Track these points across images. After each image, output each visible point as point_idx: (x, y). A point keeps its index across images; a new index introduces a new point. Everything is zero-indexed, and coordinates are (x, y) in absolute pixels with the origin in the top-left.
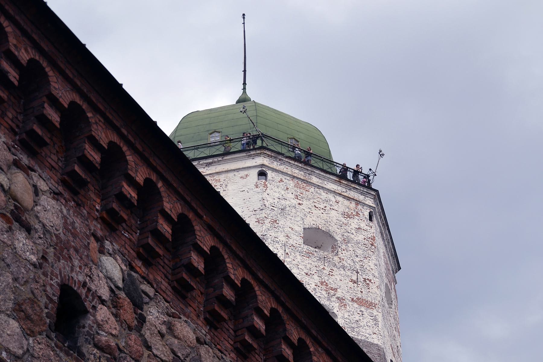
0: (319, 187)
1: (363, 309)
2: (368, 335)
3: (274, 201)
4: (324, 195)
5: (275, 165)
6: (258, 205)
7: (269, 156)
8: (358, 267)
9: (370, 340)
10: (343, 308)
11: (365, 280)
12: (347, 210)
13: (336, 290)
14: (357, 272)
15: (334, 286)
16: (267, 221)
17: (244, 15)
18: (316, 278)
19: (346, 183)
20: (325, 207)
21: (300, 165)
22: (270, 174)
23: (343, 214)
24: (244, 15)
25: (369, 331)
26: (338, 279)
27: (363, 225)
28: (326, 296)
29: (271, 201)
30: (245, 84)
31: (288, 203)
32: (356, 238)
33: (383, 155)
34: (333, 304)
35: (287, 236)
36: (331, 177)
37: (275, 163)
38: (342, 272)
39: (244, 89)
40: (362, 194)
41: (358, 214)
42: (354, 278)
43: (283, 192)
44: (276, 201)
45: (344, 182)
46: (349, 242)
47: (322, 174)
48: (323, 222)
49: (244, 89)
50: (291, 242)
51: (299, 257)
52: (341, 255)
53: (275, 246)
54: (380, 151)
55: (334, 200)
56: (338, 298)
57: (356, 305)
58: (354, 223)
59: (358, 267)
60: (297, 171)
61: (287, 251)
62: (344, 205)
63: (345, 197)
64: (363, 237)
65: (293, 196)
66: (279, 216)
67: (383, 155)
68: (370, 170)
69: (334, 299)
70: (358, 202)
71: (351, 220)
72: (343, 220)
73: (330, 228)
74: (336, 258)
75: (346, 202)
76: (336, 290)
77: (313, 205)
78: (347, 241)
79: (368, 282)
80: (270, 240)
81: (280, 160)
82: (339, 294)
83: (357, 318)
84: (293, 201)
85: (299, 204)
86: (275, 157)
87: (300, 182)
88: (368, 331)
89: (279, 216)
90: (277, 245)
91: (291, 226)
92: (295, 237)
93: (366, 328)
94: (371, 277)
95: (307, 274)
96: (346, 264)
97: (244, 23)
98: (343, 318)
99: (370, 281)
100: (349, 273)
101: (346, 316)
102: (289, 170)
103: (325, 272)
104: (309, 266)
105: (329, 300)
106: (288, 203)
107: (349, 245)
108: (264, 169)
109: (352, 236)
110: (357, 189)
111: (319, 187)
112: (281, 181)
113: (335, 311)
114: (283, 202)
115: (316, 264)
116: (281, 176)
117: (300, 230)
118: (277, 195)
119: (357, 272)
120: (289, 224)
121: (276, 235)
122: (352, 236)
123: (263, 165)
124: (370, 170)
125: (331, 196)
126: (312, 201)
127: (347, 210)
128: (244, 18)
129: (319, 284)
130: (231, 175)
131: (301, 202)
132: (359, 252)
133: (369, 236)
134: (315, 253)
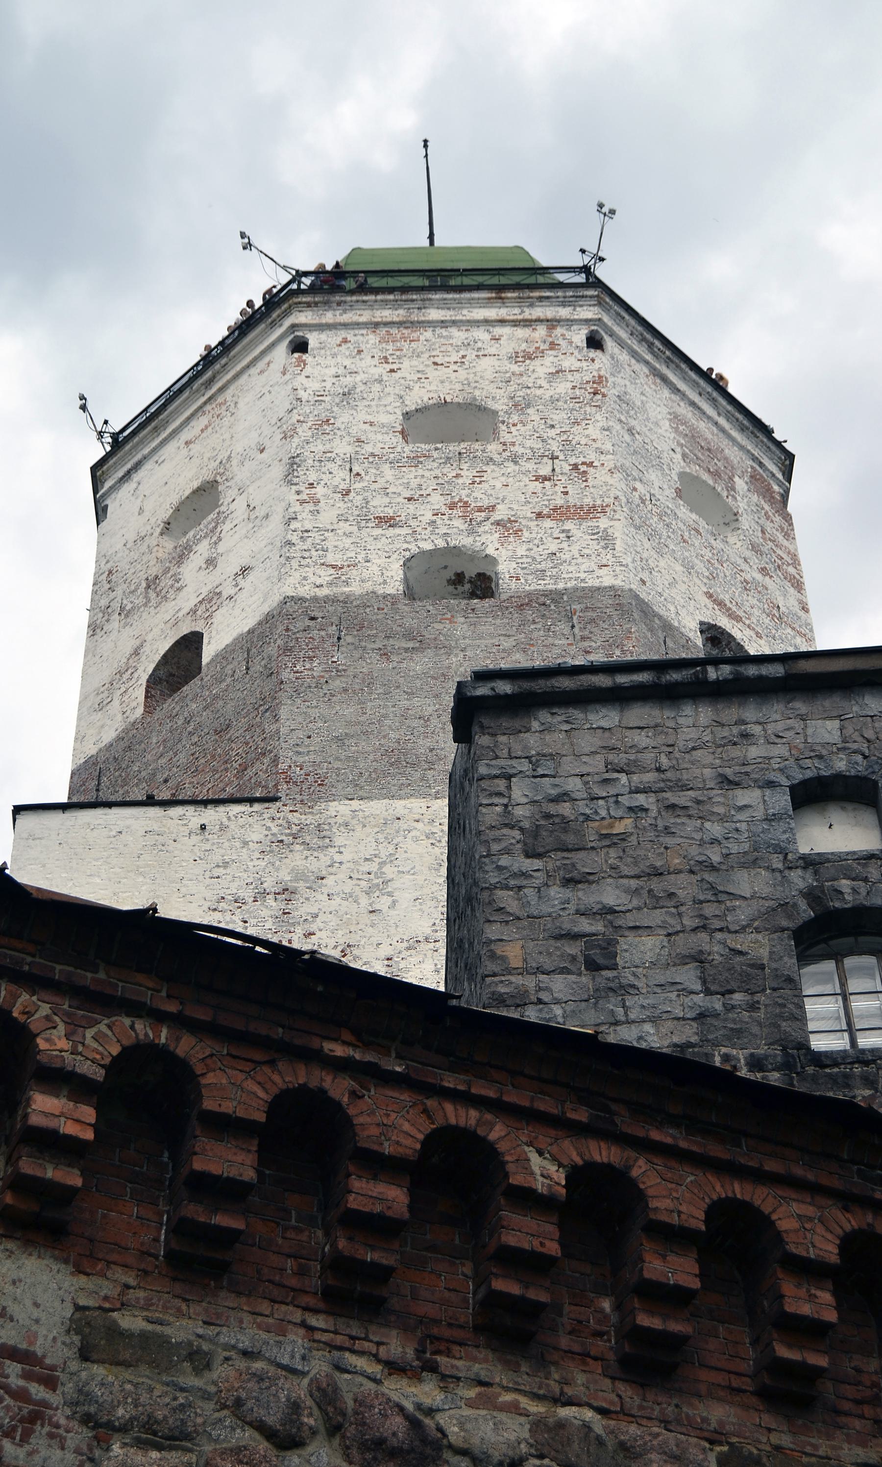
0: (443, 324)
2: (583, 575)
4: (458, 335)
7: (309, 305)
8: (554, 446)
9: (592, 582)
10: (511, 539)
11: (575, 467)
12: (524, 346)
13: (492, 508)
15: (486, 503)
17: (426, 141)
18: (437, 501)
19: (515, 295)
20: (463, 357)
21: (391, 297)
22: (313, 339)
23: (515, 357)
24: (426, 141)
25: (586, 565)
27: (569, 363)
29: (315, 385)
32: (551, 393)
33: (612, 212)
34: (483, 539)
36: (475, 295)
38: (511, 467)
40: (563, 304)
41: (553, 346)
42: (545, 471)
44: (328, 385)
45: (509, 295)
46: (528, 406)
47: (451, 296)
52: (505, 437)
53: (323, 469)
54: (601, 206)
55: (486, 336)
56: (497, 523)
57: (548, 523)
58: (542, 367)
61: (356, 468)
62: (513, 339)
64: (569, 385)
66: (335, 409)
67: (612, 212)
68: (583, 251)
69: (487, 526)
70: (552, 323)
71: (537, 362)
72: (515, 368)
73: (477, 393)
74: (493, 448)
75: (521, 332)
76: (492, 508)
77: (430, 363)
78: (520, 406)
79: (583, 468)
80: (310, 461)
83: (553, 547)
84: (373, 370)
85: (392, 371)
86: (326, 303)
87: (394, 331)
88: (583, 567)
89: (335, 409)
90: (330, 465)
91: (369, 418)
92: (380, 437)
93: (580, 560)
94: (592, 457)
95: (409, 499)
96: (520, 450)
97: (426, 156)
98: (513, 558)
100: (530, 466)
102: (365, 316)
103: (460, 481)
104: (414, 483)
105: (471, 532)
109: (539, 392)
110: (548, 298)
111: (443, 324)
112: (345, 341)
113: (490, 551)
115: (437, 472)
116: (343, 334)
117: (395, 419)
119: (553, 458)
120: (363, 416)
121: (328, 447)
122: (539, 392)
123: (294, 327)
124: (583, 251)
125: (481, 334)
126: (426, 355)
127: (524, 346)
129: (444, 509)
131: (395, 367)
132: (557, 417)
134: (435, 454)
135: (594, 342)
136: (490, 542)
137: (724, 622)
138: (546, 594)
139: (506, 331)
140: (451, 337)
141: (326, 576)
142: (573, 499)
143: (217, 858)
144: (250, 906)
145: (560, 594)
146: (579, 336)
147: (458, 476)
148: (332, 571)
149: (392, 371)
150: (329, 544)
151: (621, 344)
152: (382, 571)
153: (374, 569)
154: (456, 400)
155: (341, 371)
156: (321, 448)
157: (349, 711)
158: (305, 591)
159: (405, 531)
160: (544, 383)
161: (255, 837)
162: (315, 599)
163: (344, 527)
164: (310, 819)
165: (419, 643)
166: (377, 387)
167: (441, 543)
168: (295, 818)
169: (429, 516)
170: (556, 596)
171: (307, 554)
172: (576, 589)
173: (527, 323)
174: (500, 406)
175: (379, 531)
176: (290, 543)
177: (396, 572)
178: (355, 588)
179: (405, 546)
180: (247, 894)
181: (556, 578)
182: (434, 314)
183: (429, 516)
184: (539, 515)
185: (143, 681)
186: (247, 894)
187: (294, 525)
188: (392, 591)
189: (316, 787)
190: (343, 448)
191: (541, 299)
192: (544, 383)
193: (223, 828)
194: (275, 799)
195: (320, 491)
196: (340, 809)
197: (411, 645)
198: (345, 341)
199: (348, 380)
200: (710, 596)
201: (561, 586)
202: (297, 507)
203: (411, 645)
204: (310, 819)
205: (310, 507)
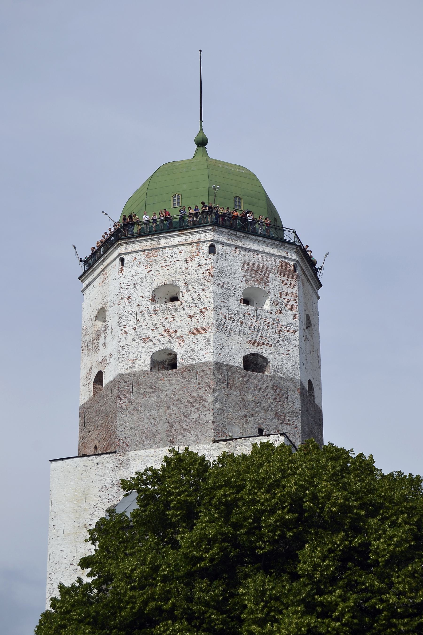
1: (198, 337)
2: (201, 357)
3: (129, 280)
5: (132, 247)
6: (118, 290)
7: (124, 243)
9: (203, 360)
10: (181, 344)
14: (196, 307)
15: (174, 329)
16: (123, 301)
18: (161, 329)
19: (187, 232)
25: (202, 353)
26: (179, 321)
27: (203, 261)
28: (168, 340)
30: (201, 121)
31: (140, 275)
32: (196, 276)
34: (172, 345)
35: (139, 305)
37: (131, 245)
39: (201, 126)
40: (202, 232)
42: (192, 313)
43: (136, 269)
44: (130, 280)
45: (185, 232)
46: (189, 284)
48: (169, 276)
49: (201, 126)
50: (142, 308)
51: (147, 318)
53: (129, 319)
56: (177, 338)
57: (192, 336)
58: (194, 264)
59: (196, 301)
60: (148, 243)
61: (138, 318)
63: (187, 244)
64: (202, 272)
65: (144, 268)
66: (132, 291)
69: (175, 339)
70: (198, 243)
71: (193, 262)
72: (186, 266)
75: (189, 248)
77: (160, 266)
78: (186, 284)
79: (204, 310)
80: (125, 316)
81: (133, 241)
82: (178, 334)
83: (193, 346)
85: (149, 272)
87: (150, 252)
88: (201, 354)
89: (132, 291)
90: (131, 317)
92: (145, 302)
93: (200, 351)
95: (153, 330)
97: (201, 60)
99: (205, 309)
101: (184, 349)
105: (170, 342)
106: (140, 275)
107: (189, 286)
108: (122, 256)
110: (197, 231)
112: (135, 259)
113: (175, 350)
114: (136, 277)
115: (161, 317)
118: (131, 274)
121: (130, 309)
122: (192, 276)
123: (120, 254)
125: (176, 250)
126: (159, 263)
128: (201, 54)
129: (163, 334)
130: (107, 270)
131: (150, 269)
132: (198, 287)
133: (207, 268)
135: (212, 249)
136: (175, 347)
137: (254, 350)
138: (190, 366)
139: (183, 248)
140: (167, 253)
141: (129, 364)
142: (200, 325)
143: (101, 473)
144: (110, 489)
145: (194, 365)
146: (206, 248)
147: (167, 318)
148: (131, 362)
149: (149, 272)
150: (130, 351)
151: (222, 244)
152: (145, 363)
153: (143, 360)
154: (168, 283)
155: (134, 273)
156: (128, 310)
157: (135, 417)
158: (123, 372)
159: (151, 343)
160: (194, 272)
161: (111, 465)
162: (126, 374)
163: (134, 344)
164: (124, 458)
165: (155, 389)
166: (144, 280)
167: (161, 348)
168: (121, 458)
169: (158, 337)
170: (192, 366)
171: (124, 356)
172: (198, 363)
173: (190, 244)
174: (180, 284)
175: (144, 344)
176: (119, 352)
177: (149, 361)
178: (137, 369)
179: (151, 350)
180: (109, 485)
181: (193, 359)
182: (163, 242)
183: (158, 337)
184: (190, 333)
185: (93, 381)
186: (109, 485)
187: (121, 344)
188: (147, 369)
189: (126, 447)
190: (134, 309)
191: (195, 232)
192: (194, 272)
193: (103, 463)
194: (115, 452)
195: (128, 328)
196: (132, 454)
197: (152, 390)
198: (135, 259)
199: (136, 277)
200: (250, 342)
201: (194, 362)
202: (121, 336)
203: (152, 390)
204: (124, 458)
205: (124, 336)
